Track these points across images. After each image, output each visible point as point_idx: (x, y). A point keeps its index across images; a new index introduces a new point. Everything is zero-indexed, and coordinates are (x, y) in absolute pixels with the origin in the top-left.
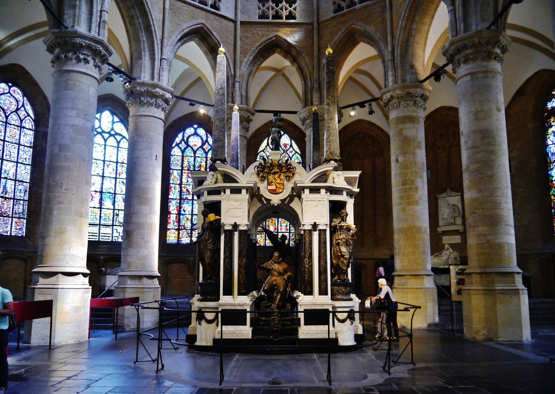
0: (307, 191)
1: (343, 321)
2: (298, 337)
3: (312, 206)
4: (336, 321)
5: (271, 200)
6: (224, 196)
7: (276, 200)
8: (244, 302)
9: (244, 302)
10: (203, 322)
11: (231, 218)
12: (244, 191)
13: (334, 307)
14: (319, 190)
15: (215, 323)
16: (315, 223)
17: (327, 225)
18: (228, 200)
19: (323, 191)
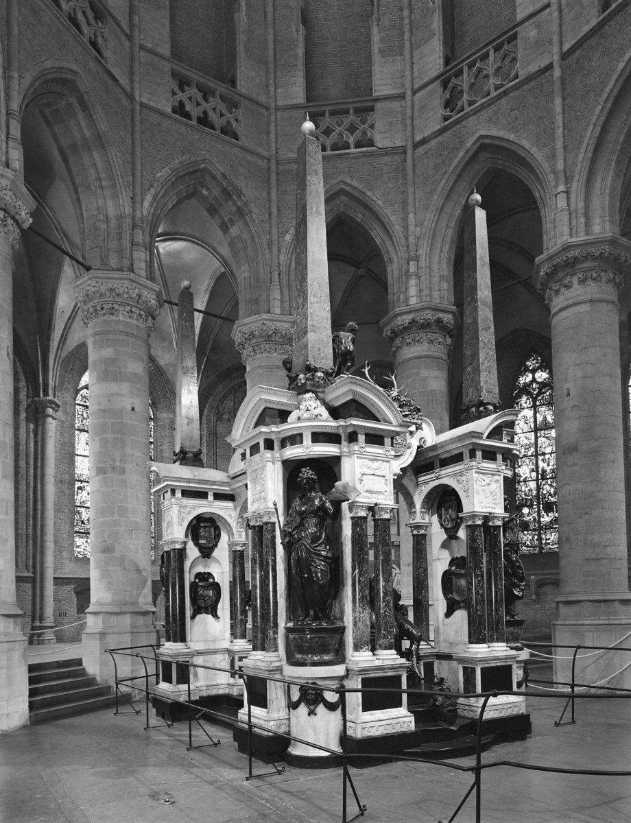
11: (368, 495)
18: (362, 456)
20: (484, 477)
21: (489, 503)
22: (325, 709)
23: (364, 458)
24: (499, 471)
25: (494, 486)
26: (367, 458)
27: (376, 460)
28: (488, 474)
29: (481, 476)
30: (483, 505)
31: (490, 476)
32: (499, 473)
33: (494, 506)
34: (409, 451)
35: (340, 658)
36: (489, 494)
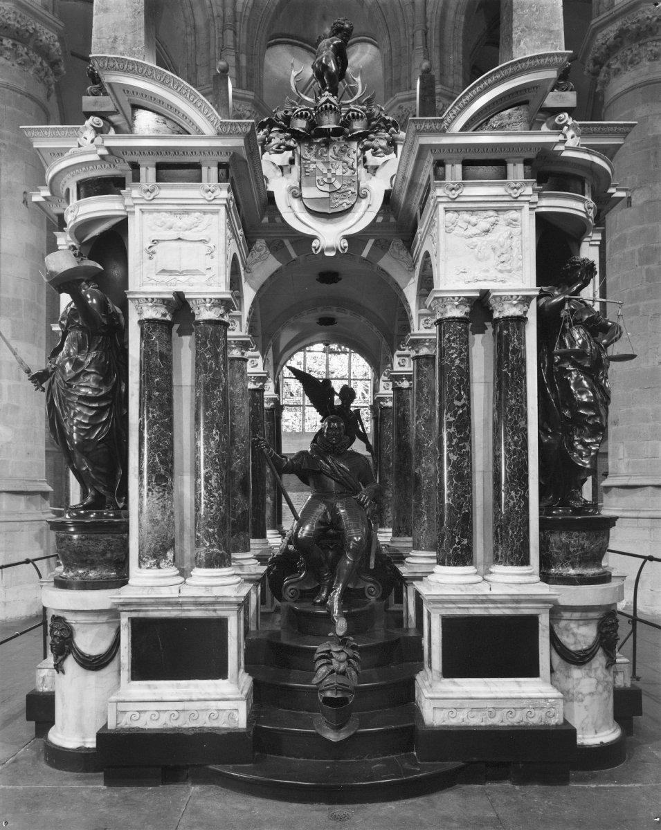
0: (454, 171)
1: (580, 659)
2: (416, 713)
3: (473, 230)
4: (557, 659)
5: (313, 238)
6: (135, 193)
7: (329, 236)
8: (218, 588)
9: (218, 588)
10: (70, 663)
11: (166, 278)
12: (211, 173)
13: (556, 611)
14: (502, 163)
15: (113, 666)
16: (485, 294)
17: (526, 300)
19: (517, 171)
20: (473, 219)
21: (487, 271)
22: (76, 665)
23: (158, 211)
24: (516, 200)
25: (501, 233)
26: (166, 211)
27: (187, 212)
28: (486, 210)
29: (466, 216)
30: (468, 277)
31: (491, 213)
32: (516, 205)
33: (500, 276)
34: (364, 203)
35: (122, 581)
36: (489, 251)
